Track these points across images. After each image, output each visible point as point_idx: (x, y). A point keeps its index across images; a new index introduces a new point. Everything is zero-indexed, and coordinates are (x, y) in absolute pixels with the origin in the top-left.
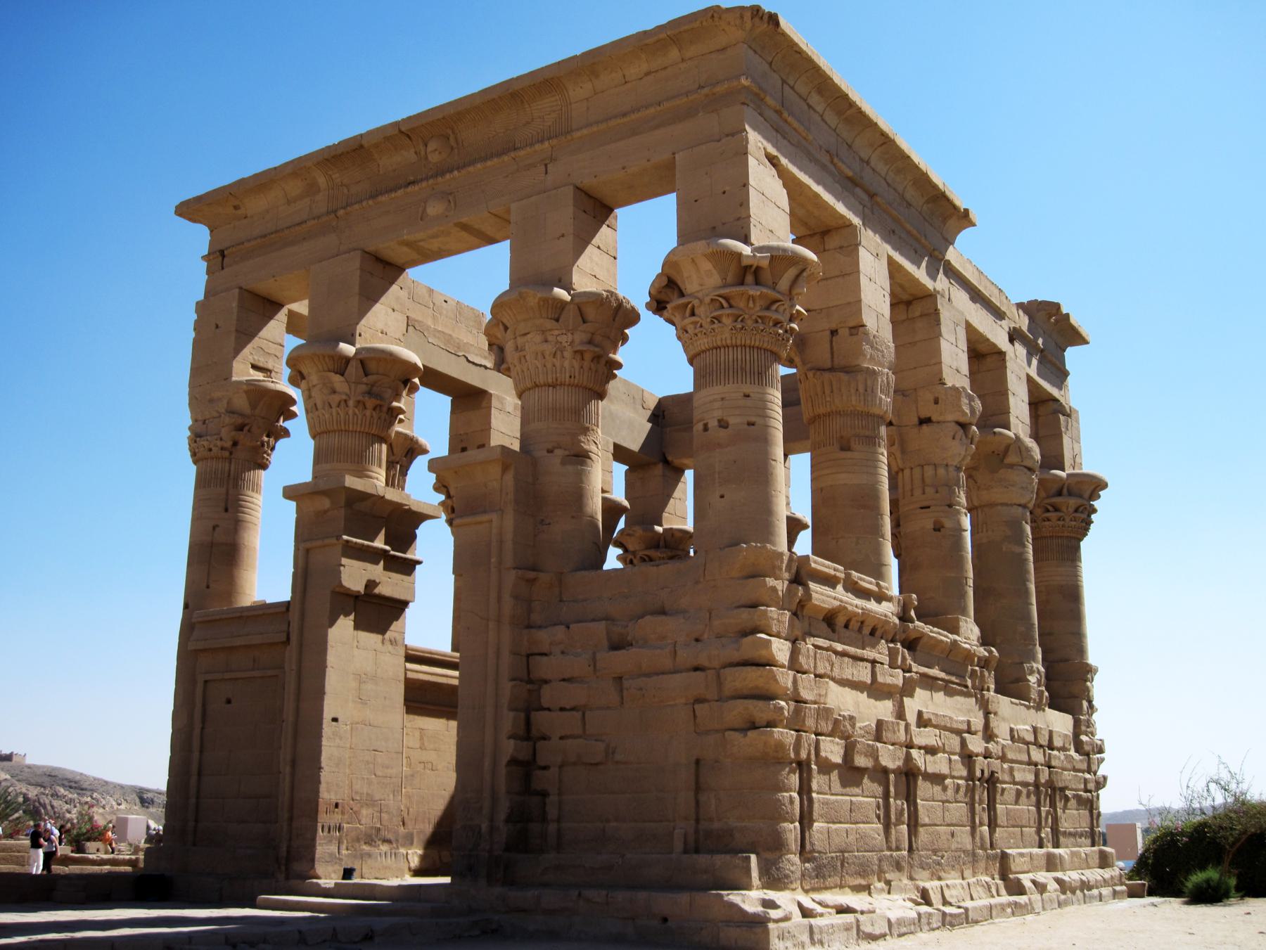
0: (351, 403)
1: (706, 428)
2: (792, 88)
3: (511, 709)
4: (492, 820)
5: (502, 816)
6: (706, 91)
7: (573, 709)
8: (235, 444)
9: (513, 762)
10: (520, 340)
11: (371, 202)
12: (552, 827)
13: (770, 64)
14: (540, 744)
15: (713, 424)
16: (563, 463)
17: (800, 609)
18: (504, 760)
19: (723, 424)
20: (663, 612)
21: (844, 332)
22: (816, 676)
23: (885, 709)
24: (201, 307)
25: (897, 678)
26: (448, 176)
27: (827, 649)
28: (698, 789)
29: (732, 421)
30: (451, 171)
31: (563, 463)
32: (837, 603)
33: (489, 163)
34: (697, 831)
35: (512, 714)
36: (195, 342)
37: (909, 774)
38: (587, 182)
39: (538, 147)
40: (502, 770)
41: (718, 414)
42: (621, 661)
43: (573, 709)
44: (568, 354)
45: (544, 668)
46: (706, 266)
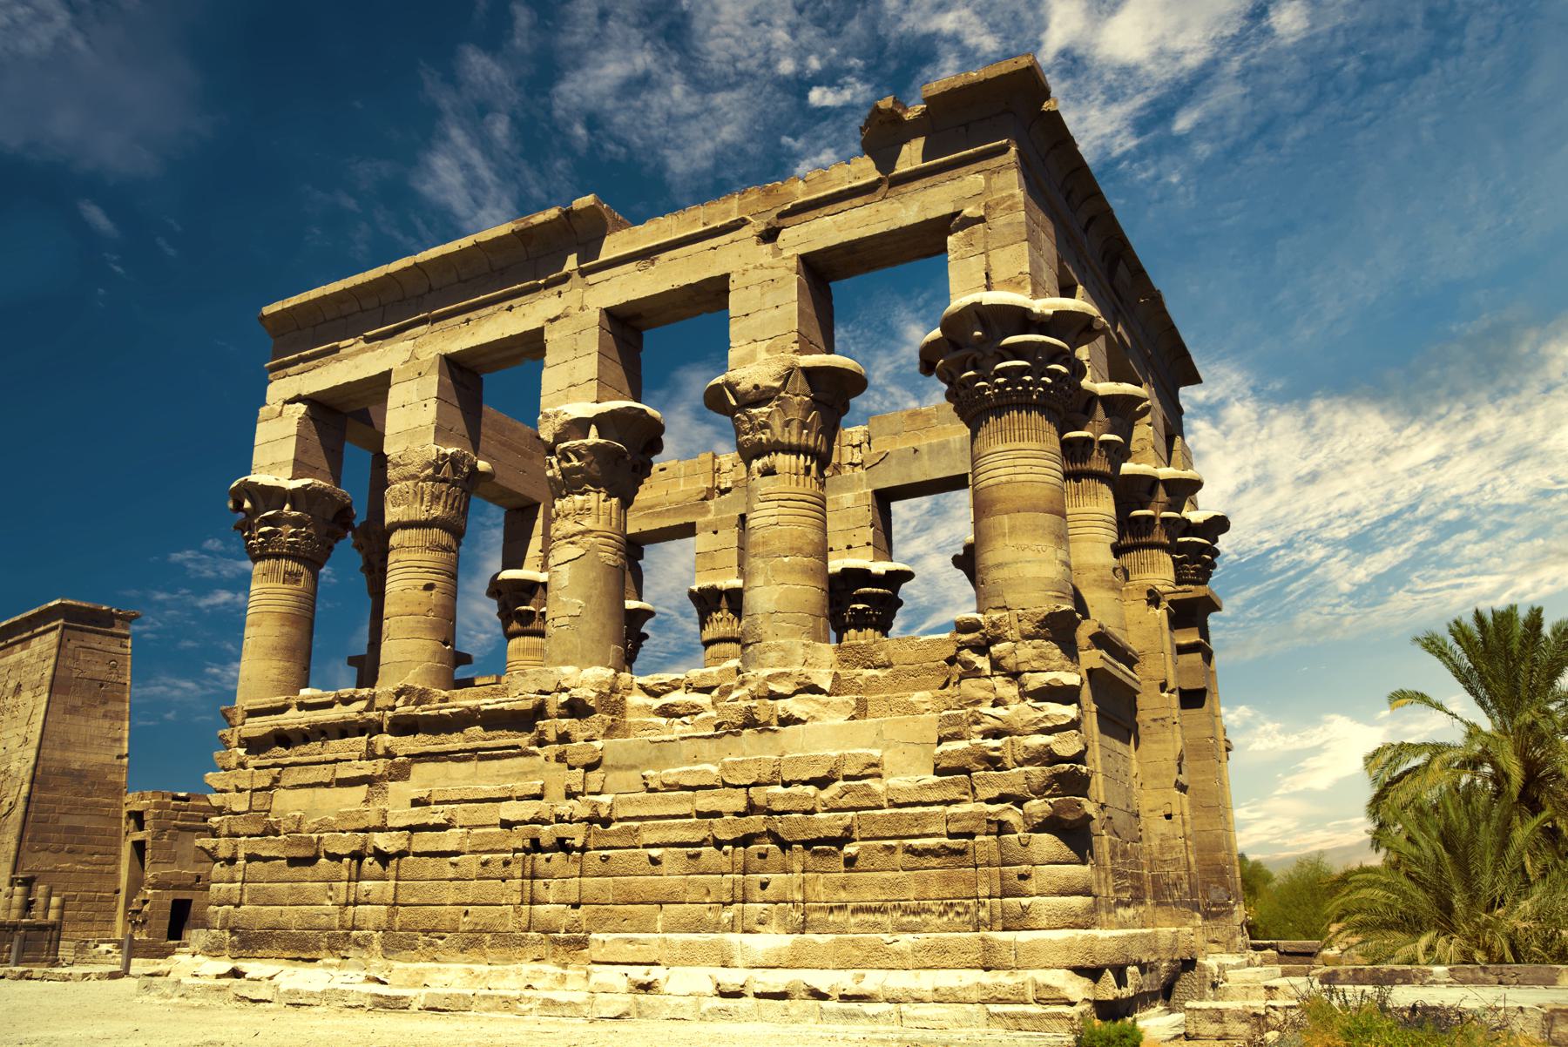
25: (380, 766)
27: (274, 766)
37: (383, 857)
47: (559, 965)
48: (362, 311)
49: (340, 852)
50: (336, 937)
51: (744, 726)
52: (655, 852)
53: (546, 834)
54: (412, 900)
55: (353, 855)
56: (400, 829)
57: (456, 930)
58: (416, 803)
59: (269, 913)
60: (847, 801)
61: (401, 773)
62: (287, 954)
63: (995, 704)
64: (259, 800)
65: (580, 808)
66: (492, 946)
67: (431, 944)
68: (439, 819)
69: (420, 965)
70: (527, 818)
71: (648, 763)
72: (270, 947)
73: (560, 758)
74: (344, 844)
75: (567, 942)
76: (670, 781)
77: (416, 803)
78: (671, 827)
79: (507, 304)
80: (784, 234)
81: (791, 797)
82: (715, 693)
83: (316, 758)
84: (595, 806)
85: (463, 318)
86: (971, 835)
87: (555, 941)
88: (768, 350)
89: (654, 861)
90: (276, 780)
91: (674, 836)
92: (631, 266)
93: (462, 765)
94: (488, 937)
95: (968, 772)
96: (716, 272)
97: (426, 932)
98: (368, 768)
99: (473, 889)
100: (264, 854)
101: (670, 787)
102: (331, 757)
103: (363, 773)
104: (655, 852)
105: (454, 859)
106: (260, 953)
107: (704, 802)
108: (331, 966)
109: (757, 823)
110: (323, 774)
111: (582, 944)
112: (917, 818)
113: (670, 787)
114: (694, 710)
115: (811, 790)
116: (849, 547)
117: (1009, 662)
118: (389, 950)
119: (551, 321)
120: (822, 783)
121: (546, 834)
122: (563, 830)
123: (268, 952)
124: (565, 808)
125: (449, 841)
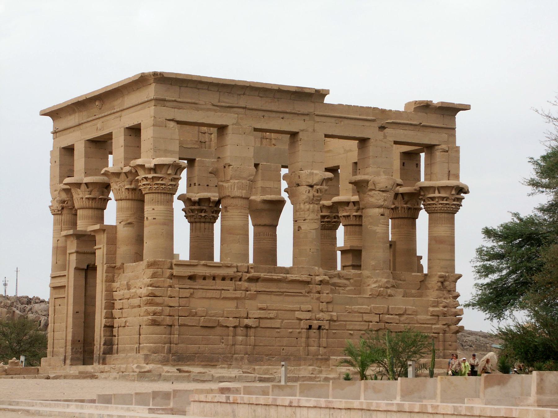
0: (84, 199)
2: (187, 87)
3: (105, 309)
4: (100, 345)
5: (102, 343)
8: (63, 208)
9: (105, 326)
13: (171, 84)
14: (115, 320)
16: (124, 227)
17: (172, 276)
18: (103, 326)
21: (227, 167)
22: (180, 298)
23: (230, 306)
24: (51, 152)
28: (140, 335)
29: (149, 218)
31: (124, 227)
32: (192, 274)
34: (139, 347)
35: (105, 311)
36: (51, 167)
38: (127, 126)
40: (102, 329)
43: (121, 309)
44: (123, 190)
45: (117, 295)
47: (318, 367)
48: (208, 90)
49: (228, 325)
50: (227, 357)
51: (378, 296)
52: (352, 332)
53: (315, 324)
54: (261, 344)
55: (235, 327)
56: (255, 318)
57: (280, 355)
58: (261, 309)
59: (193, 348)
60: (407, 321)
61: (253, 298)
62: (203, 363)
63: (445, 298)
64: (183, 302)
65: (326, 316)
66: (294, 360)
67: (269, 360)
68: (271, 316)
69: (265, 367)
70: (308, 318)
71: (347, 304)
72: (193, 360)
73: (318, 299)
74: (232, 322)
75: (322, 359)
76: (356, 310)
77: (261, 309)
78: (355, 325)
79: (282, 115)
80: (386, 130)
81: (393, 319)
82: (351, 281)
83: (212, 288)
84: (332, 316)
85: (264, 113)
86: (439, 333)
87: (317, 359)
88: (384, 172)
89: (350, 334)
90: (192, 294)
91: (357, 327)
92: (333, 120)
93: (278, 297)
94: (292, 358)
95: (438, 316)
96: (365, 136)
97: (267, 355)
98: (238, 294)
99: (285, 341)
100: (189, 324)
101: (355, 312)
102: (220, 288)
103: (236, 296)
104: (352, 332)
105: (278, 330)
106: (188, 363)
107: (366, 317)
108: (224, 368)
109: (382, 325)
110: (216, 294)
111: (327, 360)
112: (425, 328)
113: (355, 312)
114: (345, 286)
115: (397, 317)
116: (208, 186)
117: (448, 288)
118: (250, 362)
119: (302, 130)
120: (400, 315)
121: (315, 324)
122: (321, 323)
123: (193, 362)
124: (320, 315)
125: (277, 323)
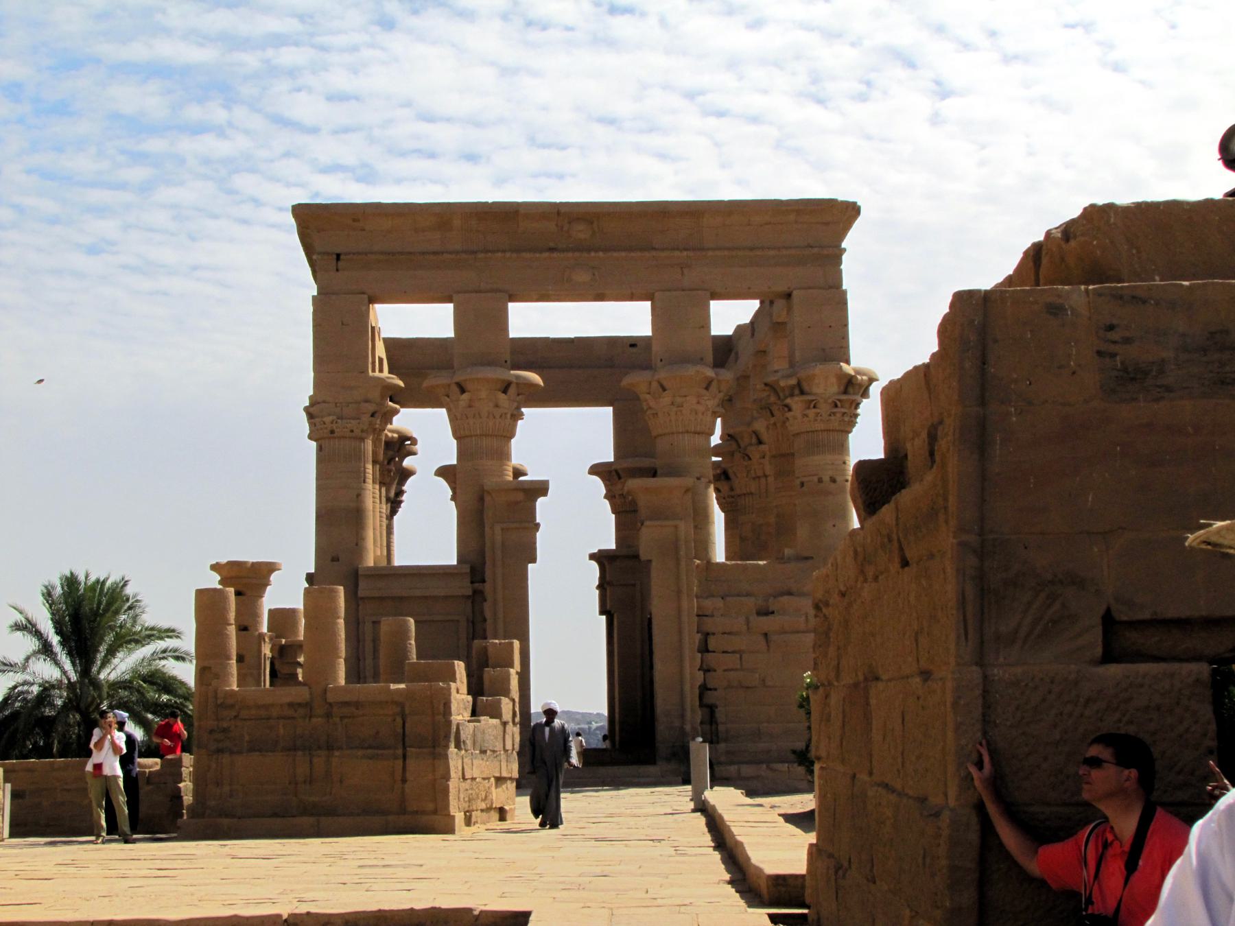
1: (820, 481)
6: (815, 250)
7: (734, 652)
10: (679, 400)
11: (514, 255)
12: (721, 728)
15: (826, 479)
19: (833, 480)
20: (790, 593)
26: (593, 254)
30: (597, 251)
33: (633, 254)
39: (677, 253)
41: (830, 473)
42: (765, 623)
43: (734, 652)
46: (834, 380)
